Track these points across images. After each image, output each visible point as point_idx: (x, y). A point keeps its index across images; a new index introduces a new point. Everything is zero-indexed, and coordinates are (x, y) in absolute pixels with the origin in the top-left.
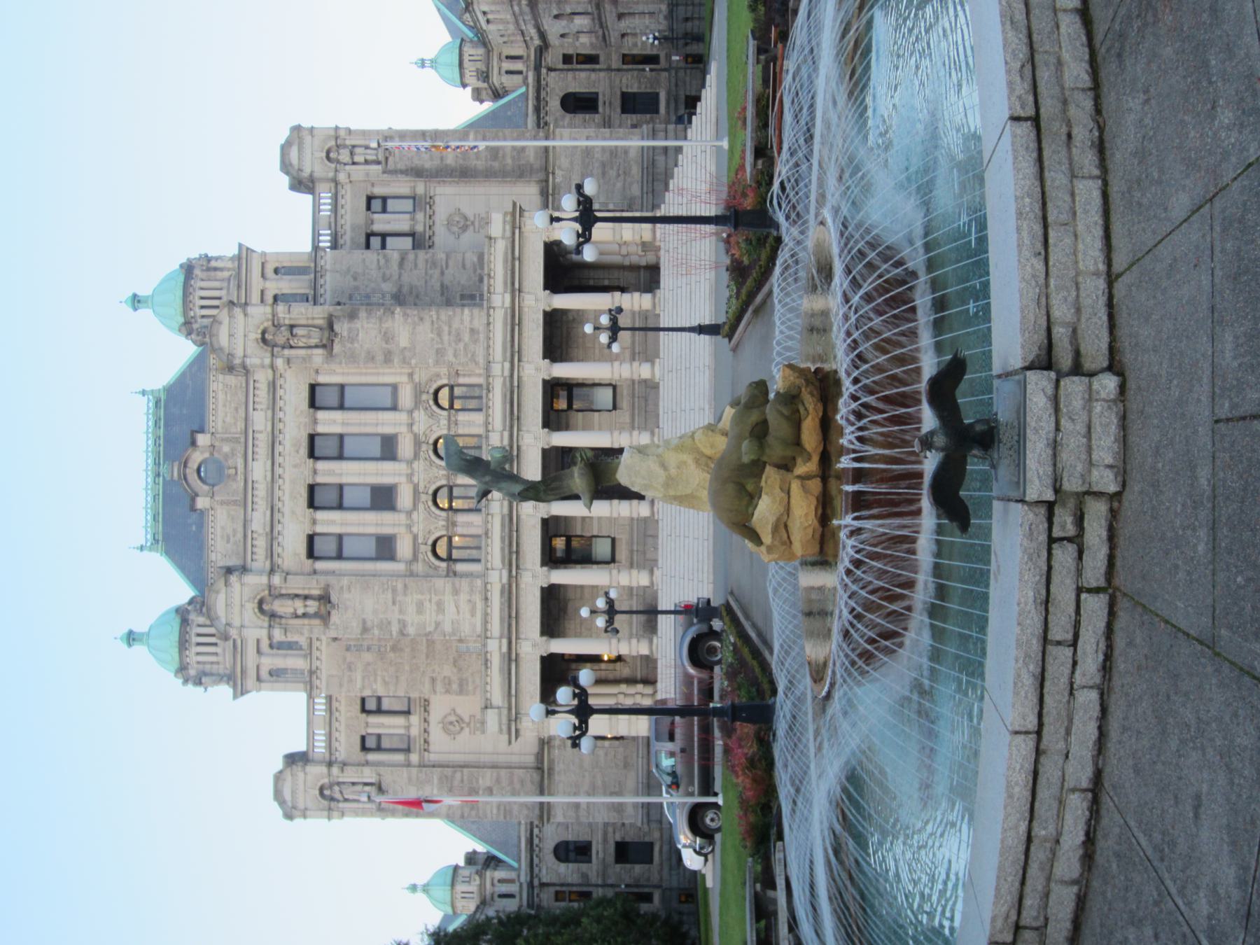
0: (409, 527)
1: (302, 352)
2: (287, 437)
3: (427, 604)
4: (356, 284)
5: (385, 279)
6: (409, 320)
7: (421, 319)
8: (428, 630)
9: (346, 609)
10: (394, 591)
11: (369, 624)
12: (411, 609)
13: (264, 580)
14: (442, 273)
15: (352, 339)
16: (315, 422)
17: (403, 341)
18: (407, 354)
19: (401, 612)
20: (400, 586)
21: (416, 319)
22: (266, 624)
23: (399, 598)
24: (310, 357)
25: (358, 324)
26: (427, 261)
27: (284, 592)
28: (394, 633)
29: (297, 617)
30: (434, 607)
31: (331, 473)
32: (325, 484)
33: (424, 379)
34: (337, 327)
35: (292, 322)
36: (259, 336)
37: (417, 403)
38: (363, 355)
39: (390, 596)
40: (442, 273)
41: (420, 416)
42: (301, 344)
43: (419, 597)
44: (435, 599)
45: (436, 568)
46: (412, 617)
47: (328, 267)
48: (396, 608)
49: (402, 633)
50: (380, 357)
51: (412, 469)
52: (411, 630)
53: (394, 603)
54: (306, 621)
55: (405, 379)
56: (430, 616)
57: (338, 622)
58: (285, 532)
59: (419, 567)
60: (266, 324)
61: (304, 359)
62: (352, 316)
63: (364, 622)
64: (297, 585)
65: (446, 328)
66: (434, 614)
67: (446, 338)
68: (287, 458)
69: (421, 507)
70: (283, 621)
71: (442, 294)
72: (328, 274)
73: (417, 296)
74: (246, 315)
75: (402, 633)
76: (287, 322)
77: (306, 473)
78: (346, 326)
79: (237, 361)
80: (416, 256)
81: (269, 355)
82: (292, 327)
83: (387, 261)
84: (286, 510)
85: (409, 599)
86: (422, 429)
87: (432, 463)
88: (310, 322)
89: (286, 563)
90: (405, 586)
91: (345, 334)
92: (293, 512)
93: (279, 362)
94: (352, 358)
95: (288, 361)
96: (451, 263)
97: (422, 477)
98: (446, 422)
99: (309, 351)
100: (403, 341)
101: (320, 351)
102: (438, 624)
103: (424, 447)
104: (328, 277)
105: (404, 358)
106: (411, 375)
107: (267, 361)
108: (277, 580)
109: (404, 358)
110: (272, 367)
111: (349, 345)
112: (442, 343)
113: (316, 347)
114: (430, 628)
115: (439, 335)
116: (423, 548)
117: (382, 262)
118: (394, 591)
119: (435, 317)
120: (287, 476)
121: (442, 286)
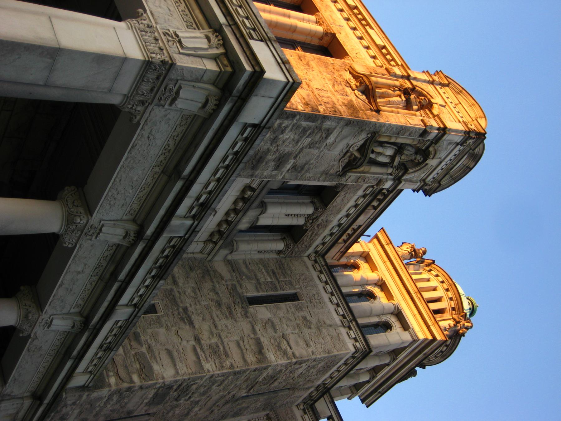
4: (301, 314)
5: (269, 323)
14: (197, 339)
26: (227, 355)
40: (197, 339)
47: (343, 331)
71: (185, 309)
72: (339, 323)
73: (219, 304)
80: (244, 359)
83: (279, 347)
91: (348, 90)
96: (191, 357)
104: (337, 319)
117: (284, 345)
121: (191, 323)
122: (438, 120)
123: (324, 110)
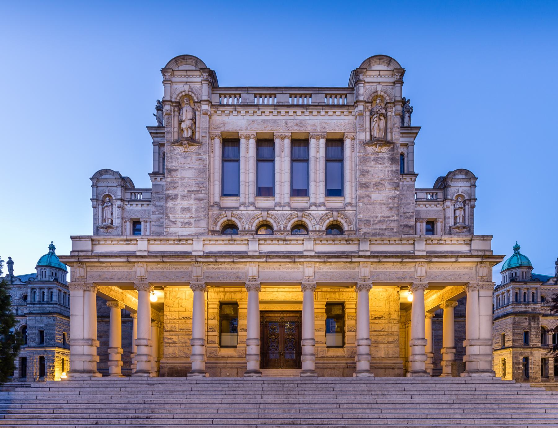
0: (243, 204)
1: (368, 125)
2: (307, 118)
3: (188, 215)
6: (390, 201)
7: (391, 209)
8: (171, 216)
9: (185, 158)
10: (198, 192)
11: (174, 174)
12: (185, 204)
13: (205, 98)
15: (376, 160)
16: (318, 138)
17: (375, 196)
18: (366, 200)
19: (184, 196)
20: (201, 196)
21: (392, 205)
22: (173, 100)
23: (193, 195)
24: (364, 130)
25: (387, 164)
27: (197, 113)
28: (168, 192)
29: (180, 124)
30: (186, 221)
31: (282, 150)
32: (274, 149)
33: (347, 214)
34: (385, 149)
35: (389, 117)
36: (379, 93)
37: (331, 210)
38: (365, 168)
39: (194, 189)
41: (322, 211)
42: (373, 124)
43: (194, 210)
44: (192, 220)
45: (215, 223)
46: (179, 204)
48: (185, 193)
49: (168, 197)
50: (364, 180)
51: (284, 206)
52: (170, 204)
53: (189, 191)
54: (176, 129)
55: (348, 200)
56: (180, 217)
57: (176, 152)
58: (240, 117)
59: (215, 211)
60: (388, 98)
61: (363, 126)
62: (393, 160)
63: (176, 170)
64: (202, 122)
65: (384, 227)
66: (181, 220)
67: (378, 227)
68: (292, 118)
69: (258, 212)
70: (177, 113)
74: (394, 83)
75: (168, 197)
76: (389, 114)
77: (281, 131)
78: (386, 156)
79: (361, 77)
81: (366, 99)
82: (385, 117)
84: (255, 117)
85: (192, 201)
86: (314, 213)
87: (289, 220)
88: (389, 130)
89: (218, 117)
90: (201, 200)
92: (253, 121)
93: (361, 108)
94: (364, 160)
95: (361, 115)
97: (279, 213)
98: (318, 229)
99: (368, 130)
100: (375, 196)
101: (368, 137)
102: (174, 223)
103: (300, 214)
105: (363, 197)
106: (350, 204)
107: (361, 98)
108: (205, 107)
109: (363, 197)
110: (357, 102)
111: (372, 159)
112: (373, 224)
113: (371, 136)
114: (172, 218)
115: (380, 222)
116: (229, 213)
118: (198, 192)
119: (391, 219)
120: (279, 117)
122: (397, 103)
123: (397, 179)
